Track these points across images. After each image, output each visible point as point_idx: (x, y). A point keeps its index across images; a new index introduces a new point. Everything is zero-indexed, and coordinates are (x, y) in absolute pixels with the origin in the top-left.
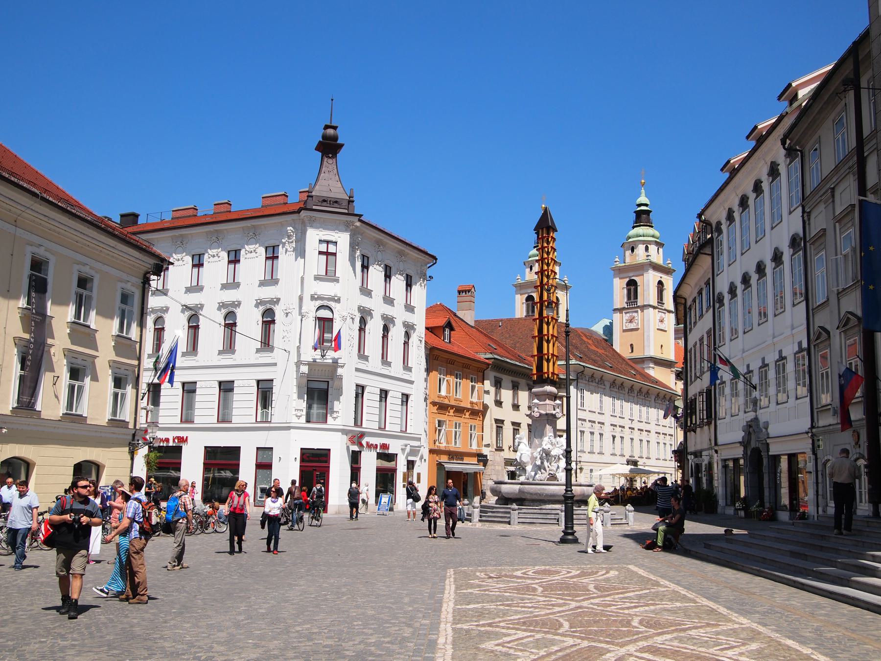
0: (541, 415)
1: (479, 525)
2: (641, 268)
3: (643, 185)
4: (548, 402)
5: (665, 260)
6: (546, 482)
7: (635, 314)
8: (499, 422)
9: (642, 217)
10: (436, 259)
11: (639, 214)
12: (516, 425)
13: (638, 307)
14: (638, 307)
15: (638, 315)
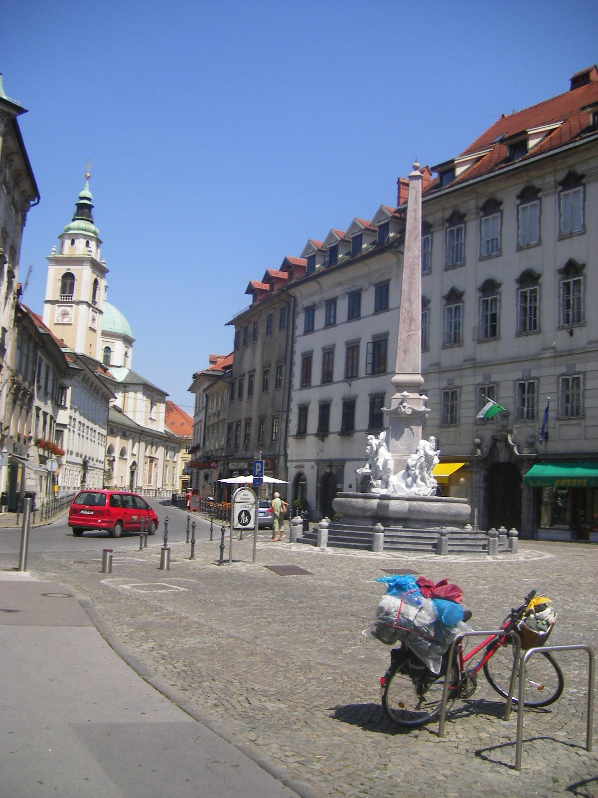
0: (414, 412)
1: (330, 551)
2: (79, 261)
3: (88, 178)
4: (416, 395)
5: (101, 259)
6: (429, 497)
7: (68, 309)
8: (38, 409)
9: (84, 210)
10: (39, 198)
11: (80, 207)
12: (45, 414)
13: (74, 302)
14: (74, 302)
15: (72, 310)
